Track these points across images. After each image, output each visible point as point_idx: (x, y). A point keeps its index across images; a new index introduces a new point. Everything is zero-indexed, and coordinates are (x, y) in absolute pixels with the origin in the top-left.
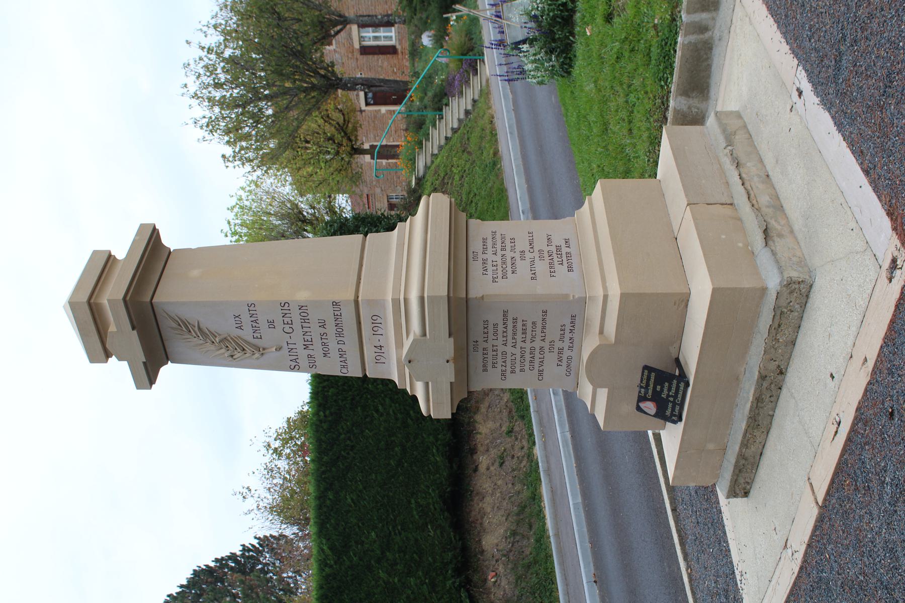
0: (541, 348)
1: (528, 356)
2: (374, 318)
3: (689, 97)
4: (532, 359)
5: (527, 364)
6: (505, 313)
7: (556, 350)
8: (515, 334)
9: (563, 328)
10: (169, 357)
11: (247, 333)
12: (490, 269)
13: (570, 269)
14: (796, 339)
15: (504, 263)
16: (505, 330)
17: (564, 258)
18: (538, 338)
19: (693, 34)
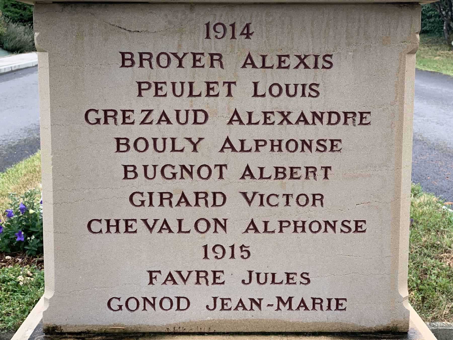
4: (175, 200)
9: (298, 279)
16: (293, 118)
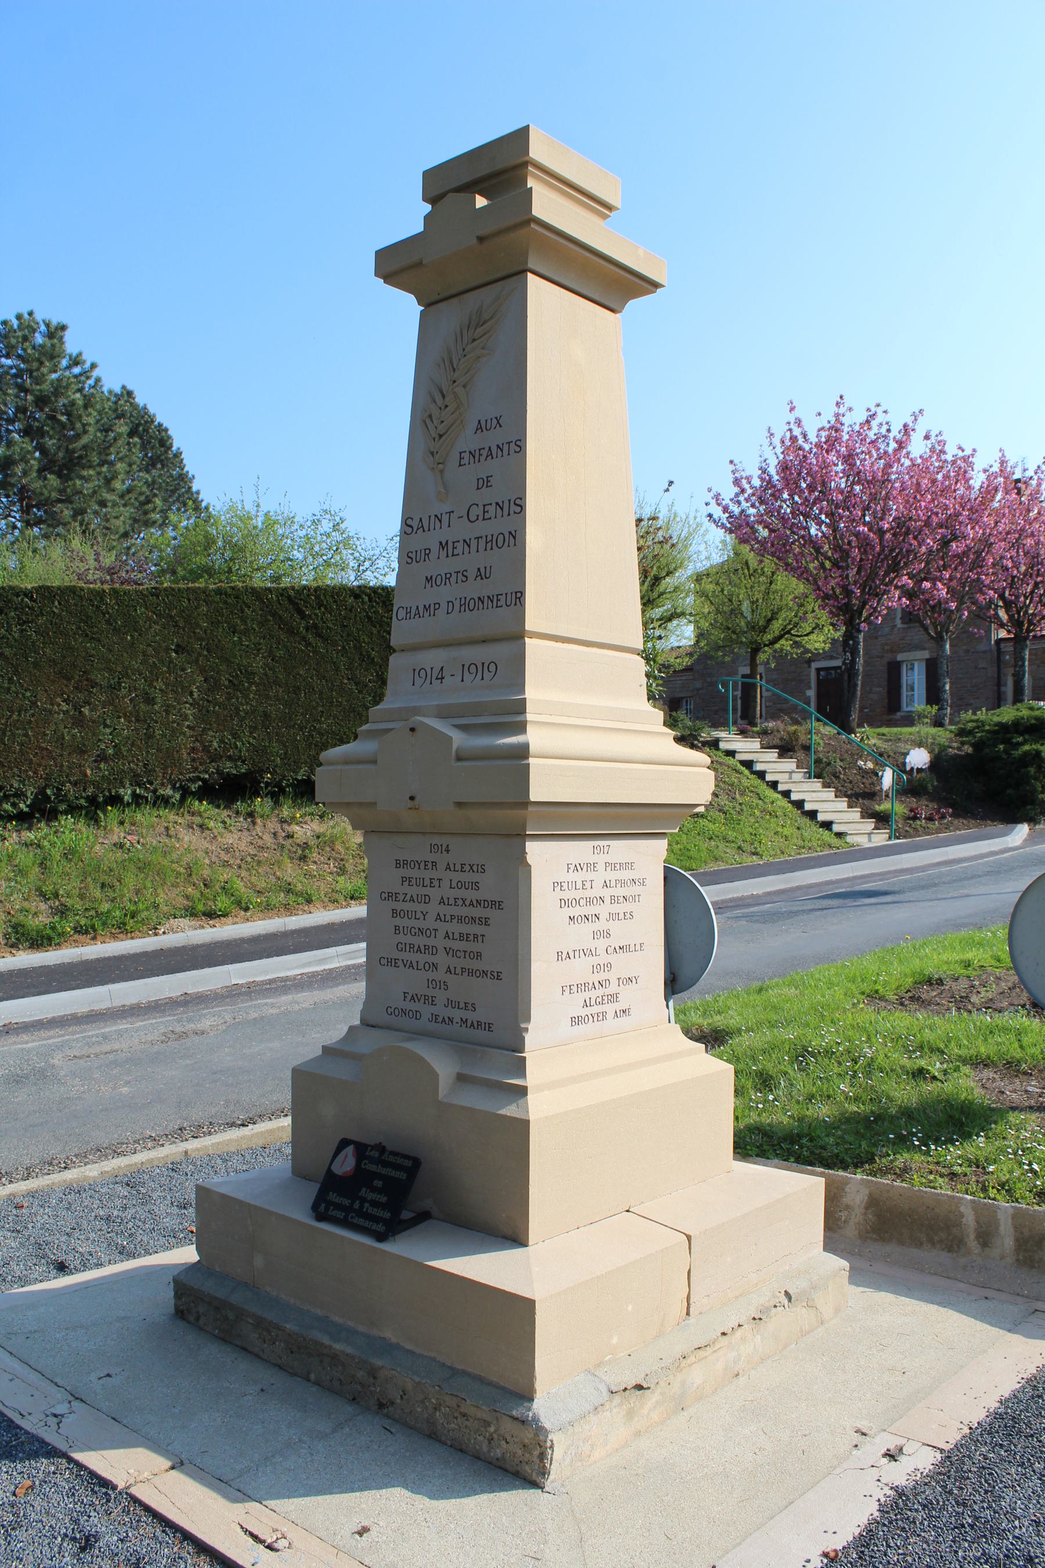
0: (435, 966)
1: (420, 941)
2: (492, 667)
3: (866, 1208)
5: (409, 939)
6: (496, 905)
7: (430, 992)
8: (460, 919)
10: (433, 308)
11: (467, 440)
12: (578, 877)
13: (576, 1021)
14: (440, 1441)
15: (590, 901)
16: (467, 903)
17: (595, 1009)
18: (453, 962)
19: (977, 1222)
